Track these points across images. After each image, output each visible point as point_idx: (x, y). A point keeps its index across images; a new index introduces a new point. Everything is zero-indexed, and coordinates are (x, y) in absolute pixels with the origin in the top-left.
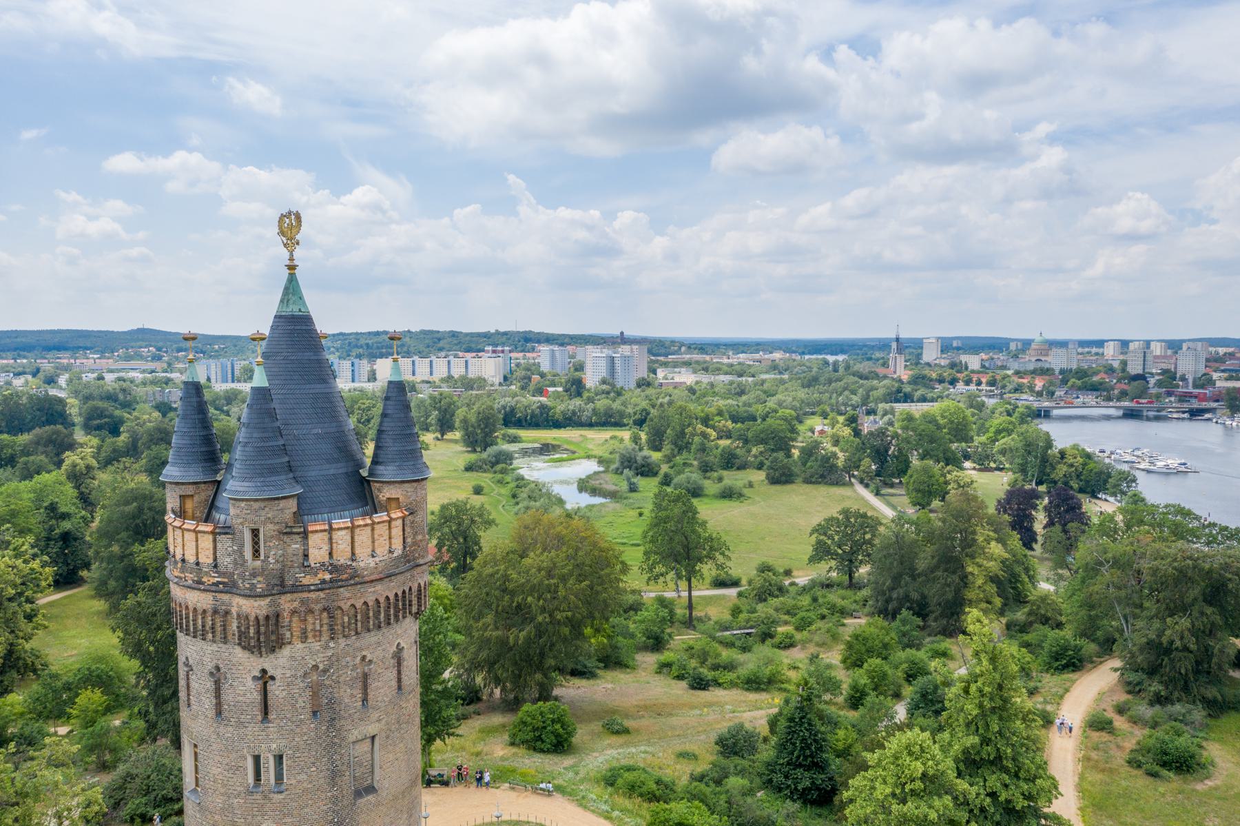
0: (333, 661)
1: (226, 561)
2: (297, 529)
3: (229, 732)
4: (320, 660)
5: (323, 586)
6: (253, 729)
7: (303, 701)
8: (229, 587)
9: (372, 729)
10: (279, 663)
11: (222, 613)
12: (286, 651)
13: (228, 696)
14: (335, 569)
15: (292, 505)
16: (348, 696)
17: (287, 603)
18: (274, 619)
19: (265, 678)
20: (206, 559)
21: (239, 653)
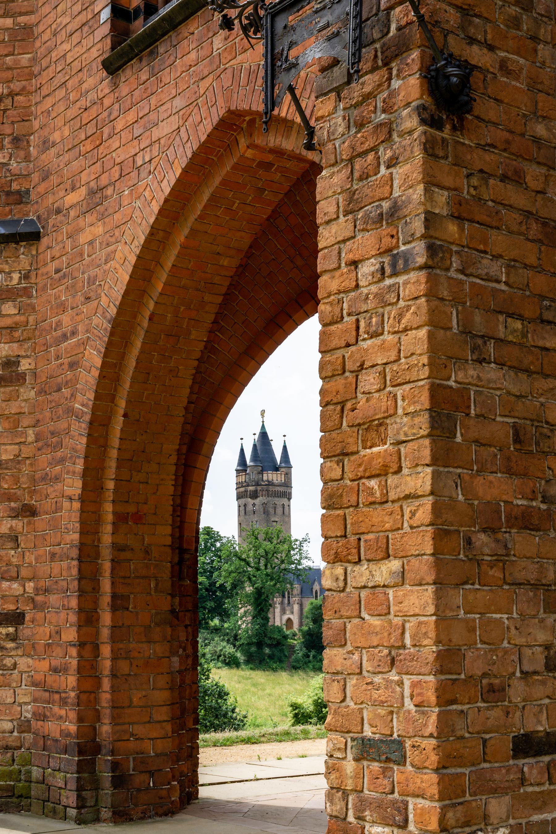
0: (268, 502)
1: (247, 480)
2: (261, 472)
3: (247, 517)
4: (265, 501)
5: (266, 485)
6: (252, 516)
7: (262, 510)
8: (248, 486)
9: (277, 520)
10: (257, 501)
11: (246, 491)
12: (259, 499)
13: (247, 509)
14: (268, 481)
15: (260, 468)
16: (271, 511)
17: (259, 488)
18: (256, 491)
19: (254, 505)
20: (243, 480)
21: (249, 499)
